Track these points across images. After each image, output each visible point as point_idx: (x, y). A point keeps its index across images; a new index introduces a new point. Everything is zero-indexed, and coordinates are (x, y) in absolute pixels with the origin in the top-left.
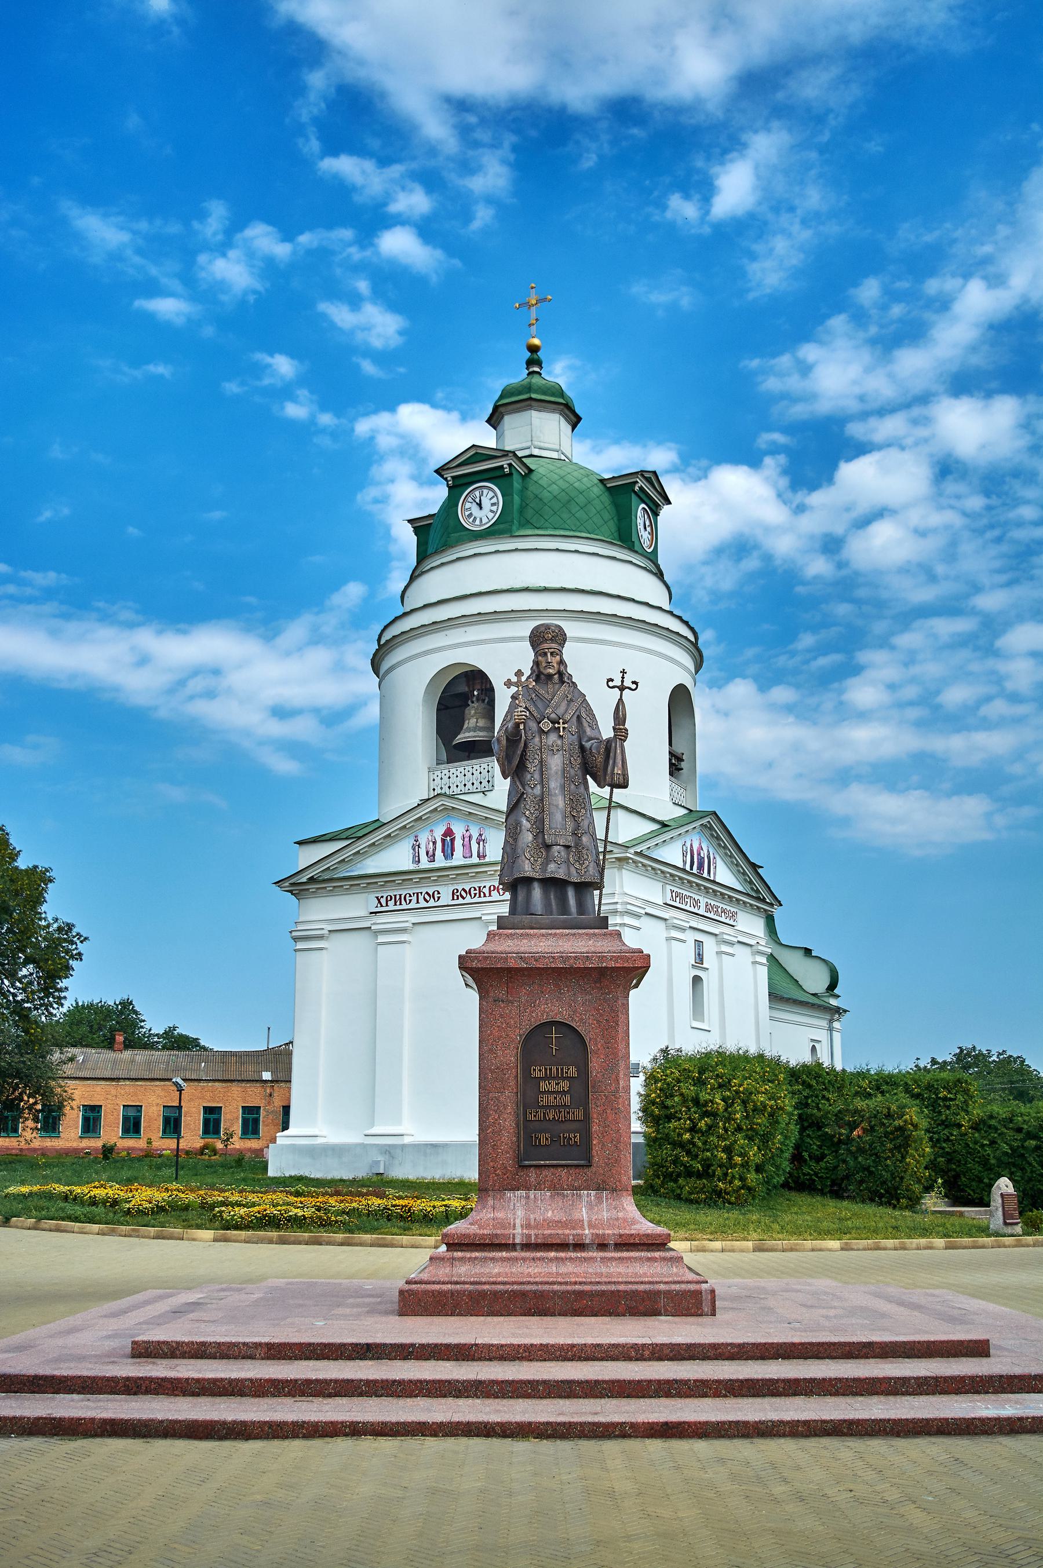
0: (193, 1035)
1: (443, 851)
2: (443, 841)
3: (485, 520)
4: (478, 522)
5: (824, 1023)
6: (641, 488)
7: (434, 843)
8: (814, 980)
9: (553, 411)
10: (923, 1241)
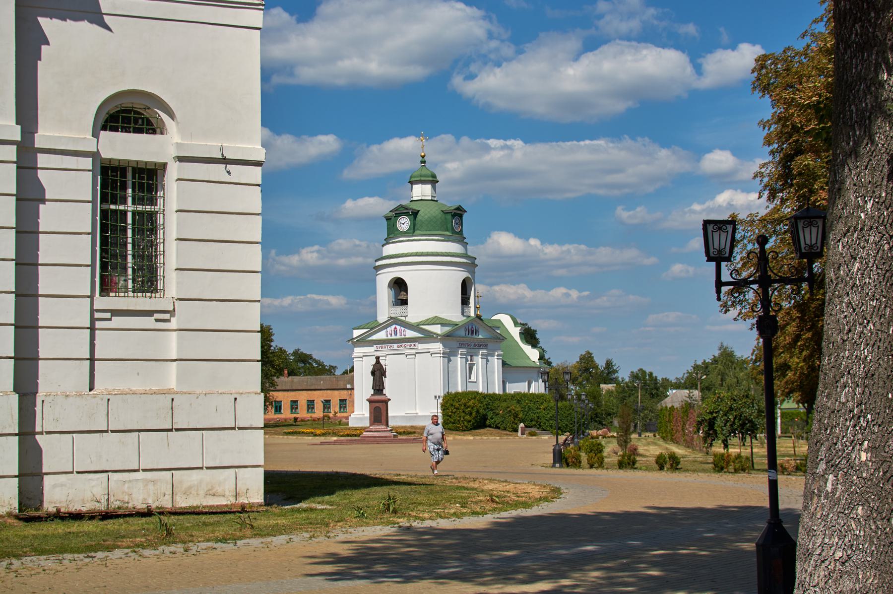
0: (308, 353)
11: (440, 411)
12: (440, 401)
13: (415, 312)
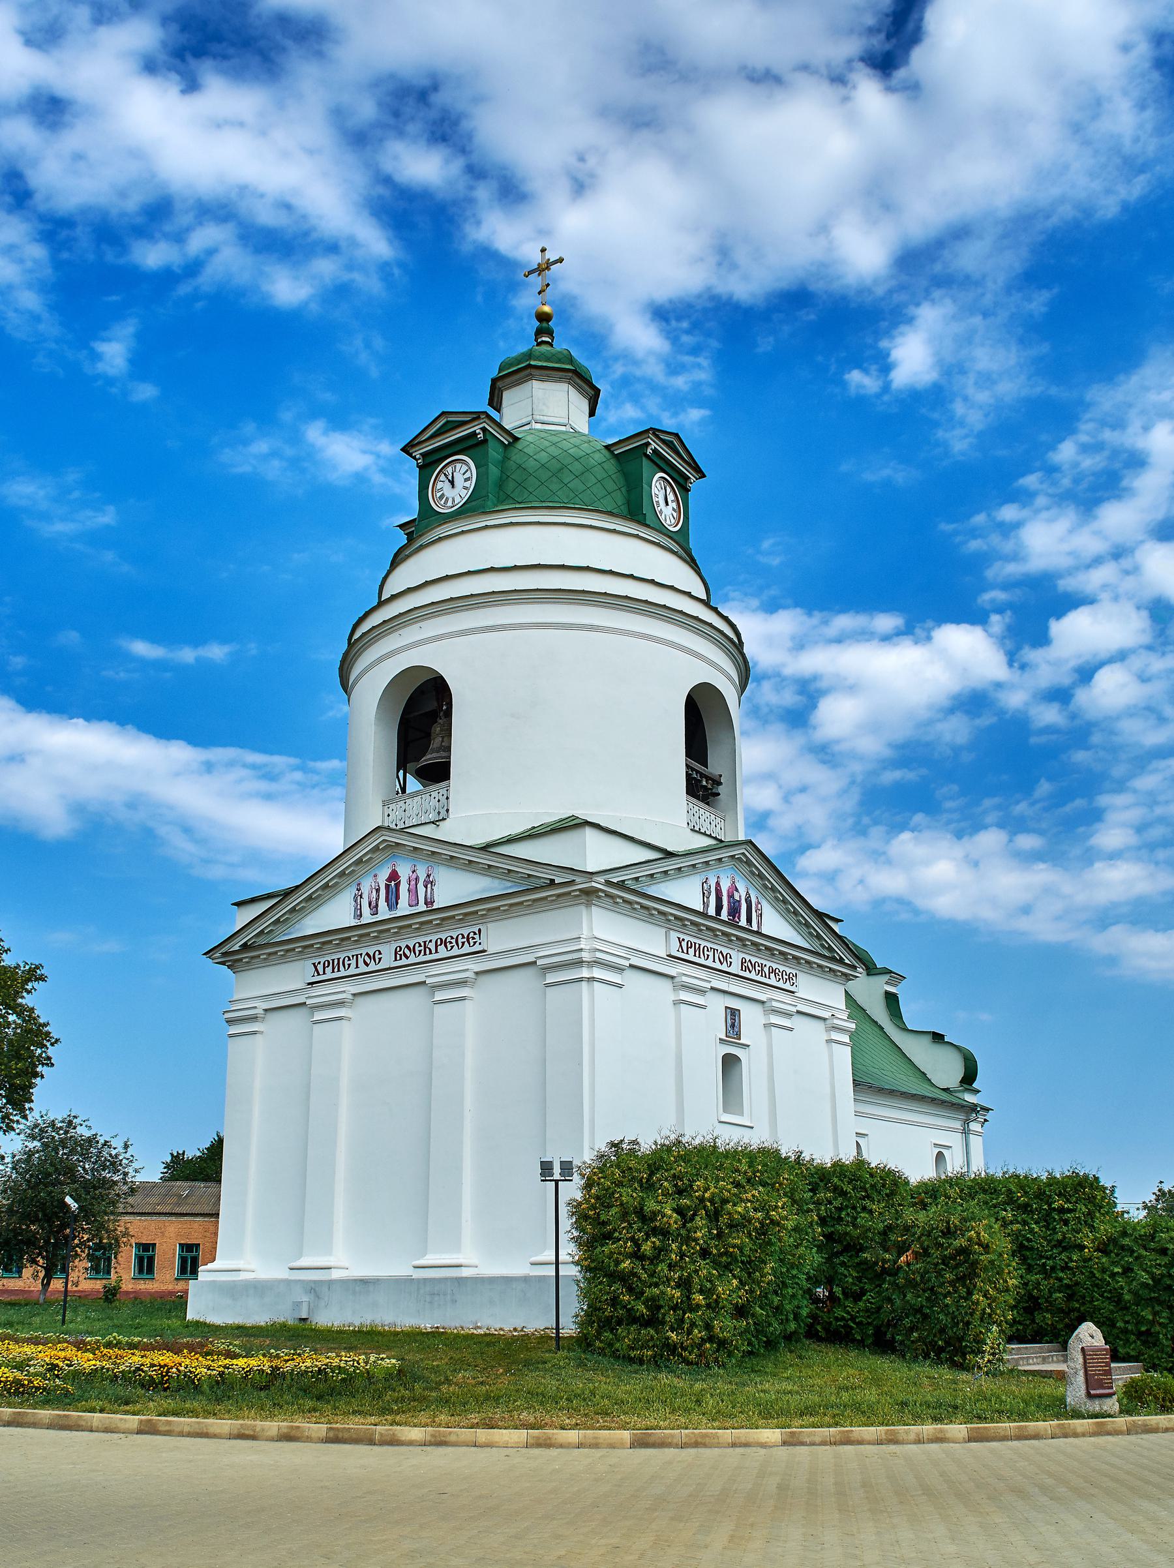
1: (387, 900)
2: (387, 887)
3: (457, 499)
4: (449, 504)
5: (958, 1125)
6: (655, 451)
7: (378, 891)
8: (944, 1071)
9: (559, 380)
10: (929, 1429)
11: (569, 1250)
12: (573, 1190)
13: (482, 802)
